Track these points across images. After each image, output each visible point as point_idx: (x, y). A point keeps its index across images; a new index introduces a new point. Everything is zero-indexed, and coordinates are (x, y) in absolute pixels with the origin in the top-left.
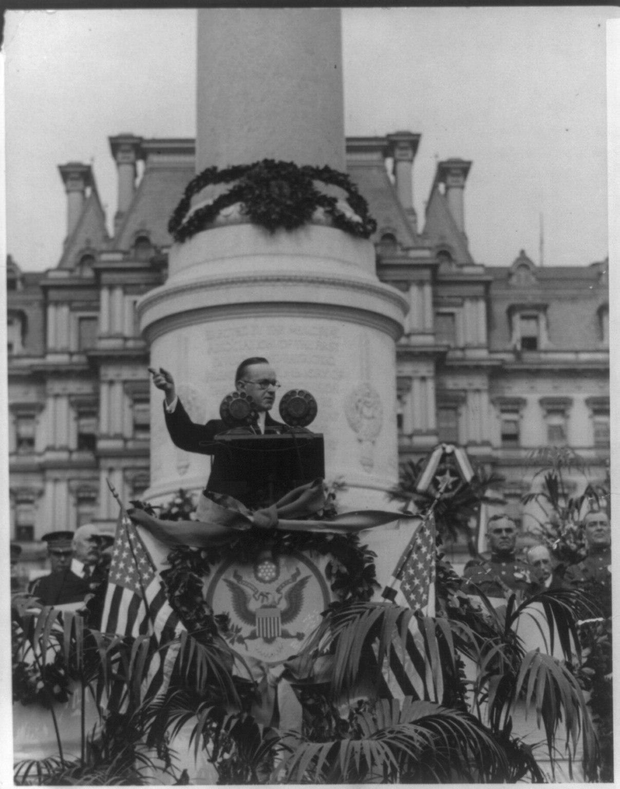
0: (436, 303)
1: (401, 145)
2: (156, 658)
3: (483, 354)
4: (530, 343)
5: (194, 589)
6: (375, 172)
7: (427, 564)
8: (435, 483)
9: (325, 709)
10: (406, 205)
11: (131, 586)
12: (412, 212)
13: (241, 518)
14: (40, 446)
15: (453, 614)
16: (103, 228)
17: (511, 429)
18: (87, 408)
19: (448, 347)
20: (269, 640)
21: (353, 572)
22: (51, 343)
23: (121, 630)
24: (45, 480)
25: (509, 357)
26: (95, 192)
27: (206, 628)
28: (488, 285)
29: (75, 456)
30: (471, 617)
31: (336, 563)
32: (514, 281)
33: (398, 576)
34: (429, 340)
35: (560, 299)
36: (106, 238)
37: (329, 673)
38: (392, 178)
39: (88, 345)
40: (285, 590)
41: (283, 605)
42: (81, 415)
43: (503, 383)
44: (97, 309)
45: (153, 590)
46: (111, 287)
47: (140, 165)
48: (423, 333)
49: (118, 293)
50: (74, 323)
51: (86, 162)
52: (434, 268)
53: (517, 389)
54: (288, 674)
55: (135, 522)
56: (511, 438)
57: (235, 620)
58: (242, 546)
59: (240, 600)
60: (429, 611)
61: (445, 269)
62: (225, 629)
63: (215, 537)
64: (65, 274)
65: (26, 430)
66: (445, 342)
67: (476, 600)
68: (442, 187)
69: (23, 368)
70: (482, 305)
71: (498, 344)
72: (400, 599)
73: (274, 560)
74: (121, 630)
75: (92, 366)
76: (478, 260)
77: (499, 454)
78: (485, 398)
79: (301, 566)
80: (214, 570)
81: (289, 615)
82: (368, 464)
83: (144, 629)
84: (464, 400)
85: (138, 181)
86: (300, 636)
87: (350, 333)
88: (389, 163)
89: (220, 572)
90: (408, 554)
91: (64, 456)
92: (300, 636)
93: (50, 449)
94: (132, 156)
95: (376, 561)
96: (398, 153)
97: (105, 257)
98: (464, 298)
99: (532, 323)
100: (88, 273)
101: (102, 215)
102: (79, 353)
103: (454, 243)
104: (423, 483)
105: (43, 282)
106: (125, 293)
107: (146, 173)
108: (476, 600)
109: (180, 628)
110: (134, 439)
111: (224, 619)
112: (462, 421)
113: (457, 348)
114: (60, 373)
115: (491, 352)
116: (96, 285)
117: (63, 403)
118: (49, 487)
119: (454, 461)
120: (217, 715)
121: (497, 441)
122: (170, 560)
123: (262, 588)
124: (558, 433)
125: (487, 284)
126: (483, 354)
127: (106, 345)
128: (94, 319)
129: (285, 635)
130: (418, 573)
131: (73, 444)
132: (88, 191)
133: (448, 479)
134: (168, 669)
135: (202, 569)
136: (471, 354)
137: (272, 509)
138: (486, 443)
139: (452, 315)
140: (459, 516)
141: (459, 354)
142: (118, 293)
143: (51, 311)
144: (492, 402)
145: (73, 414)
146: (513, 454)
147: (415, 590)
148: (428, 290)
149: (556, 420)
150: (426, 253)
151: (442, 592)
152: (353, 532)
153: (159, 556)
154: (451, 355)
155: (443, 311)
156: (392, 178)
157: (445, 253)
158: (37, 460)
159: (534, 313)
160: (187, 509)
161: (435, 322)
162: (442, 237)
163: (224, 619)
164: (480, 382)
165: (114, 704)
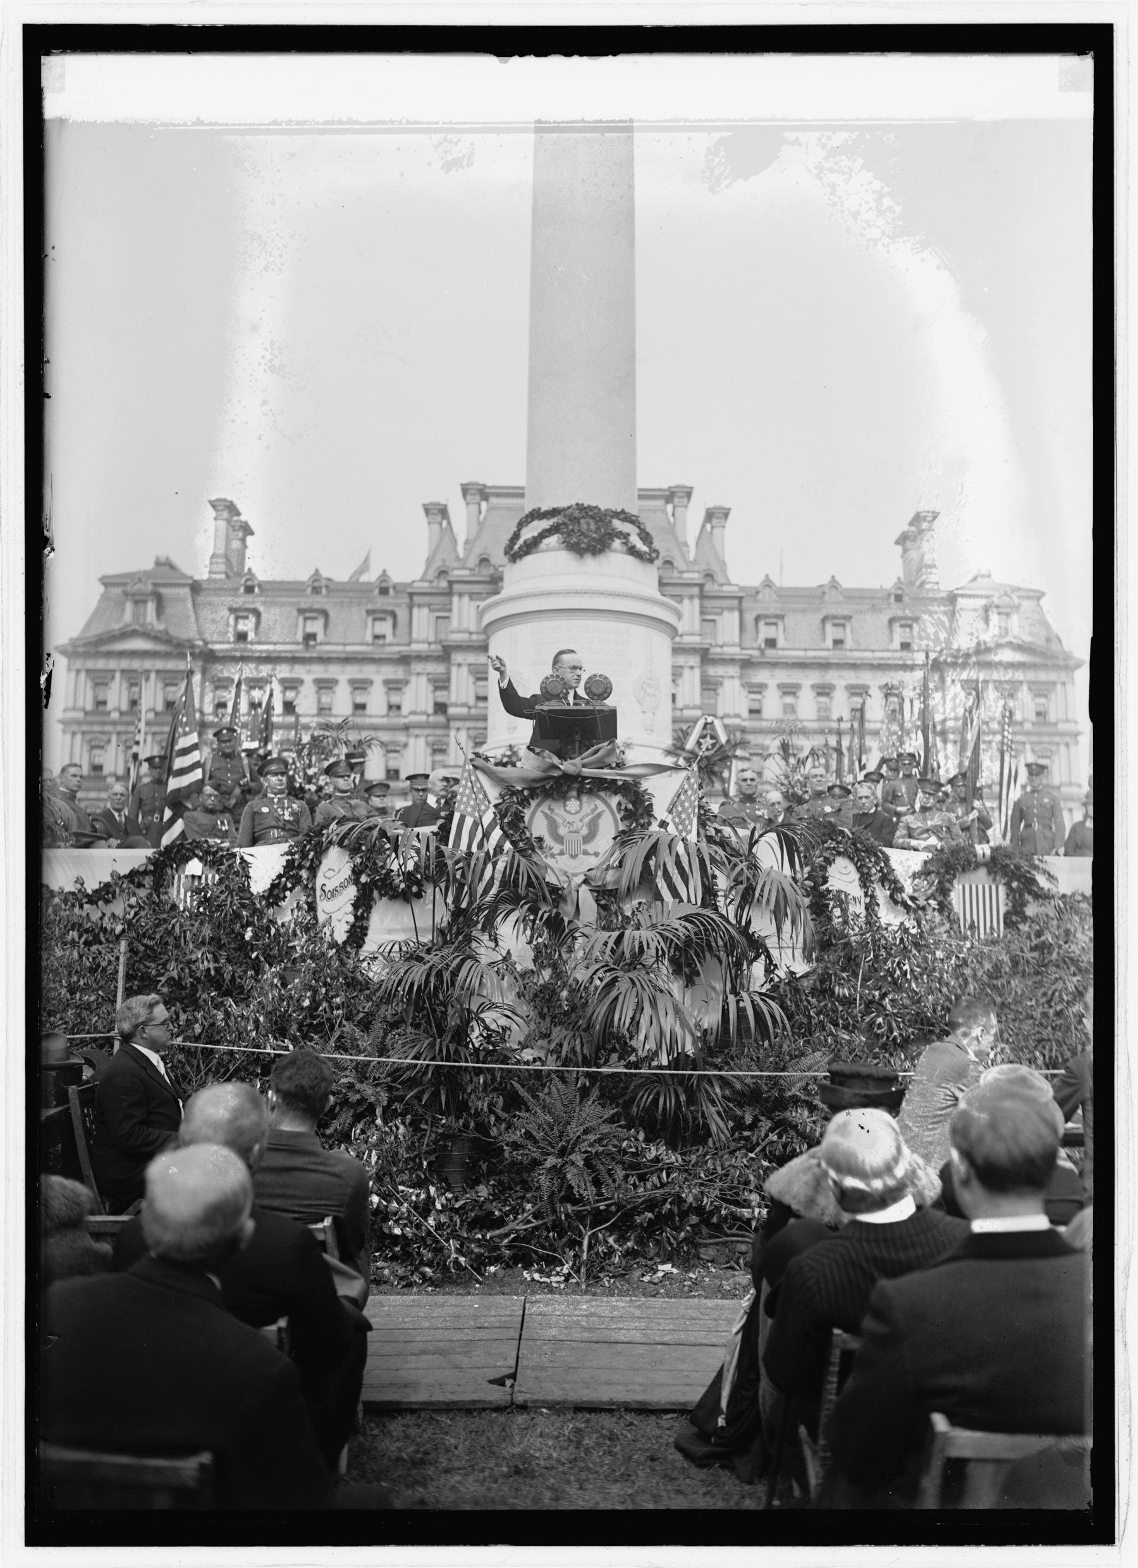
0: (702, 613)
2: (490, 867)
3: (737, 650)
4: (771, 643)
5: (519, 817)
6: (659, 514)
7: (691, 803)
8: (699, 744)
9: (614, 908)
10: (681, 539)
12: (686, 544)
13: (554, 767)
14: (405, 710)
15: (710, 840)
16: (456, 552)
17: (756, 706)
18: (441, 684)
20: (574, 857)
21: (637, 808)
22: (415, 635)
23: (463, 846)
24: (408, 736)
25: (755, 653)
26: (449, 523)
27: (527, 846)
29: (432, 719)
30: (723, 843)
31: (624, 802)
32: (760, 596)
33: (670, 812)
34: (697, 639)
35: (795, 611)
36: (457, 558)
37: (618, 881)
38: (672, 519)
39: (443, 637)
41: (585, 831)
42: (436, 688)
43: (750, 672)
44: (450, 610)
45: (488, 818)
46: (461, 595)
47: (484, 504)
49: (466, 599)
50: (433, 620)
51: (443, 502)
52: (701, 586)
53: (760, 676)
54: (586, 882)
56: (755, 712)
57: (548, 841)
58: (555, 787)
59: (553, 826)
60: (692, 838)
61: (710, 587)
62: (541, 848)
63: (534, 780)
64: (426, 584)
65: (395, 699)
66: (709, 641)
67: (727, 831)
68: (708, 526)
69: (394, 654)
70: (736, 614)
71: (747, 644)
72: (671, 828)
73: (578, 798)
74: (463, 846)
75: (445, 654)
76: (733, 581)
77: (747, 724)
78: (737, 682)
79: (598, 802)
80: (534, 803)
81: (588, 839)
82: (650, 730)
83: (481, 846)
84: (721, 684)
85: (482, 517)
86: (596, 854)
87: (639, 633)
88: (670, 507)
89: (538, 805)
91: (423, 718)
92: (596, 854)
93: (412, 713)
94: (478, 498)
95: (654, 801)
96: (676, 500)
97: (456, 572)
98: (723, 609)
99: (773, 628)
100: (444, 584)
101: (455, 542)
102: (435, 643)
103: (715, 568)
104: (690, 744)
105: (409, 590)
106: (471, 599)
107: (488, 511)
108: (727, 831)
109: (508, 846)
110: (476, 707)
111: (540, 840)
112: (720, 698)
113: (717, 646)
114: (421, 658)
116: (449, 593)
117: (423, 679)
118: (412, 741)
119: (714, 729)
120: (534, 910)
121: (745, 714)
122: (502, 796)
123: (569, 818)
124: (790, 709)
125: (740, 599)
128: (448, 618)
129: (586, 853)
130: (685, 810)
131: (430, 710)
132: (445, 523)
133: (708, 742)
134: (498, 876)
135: (524, 802)
136: (726, 650)
137: (578, 761)
138: (737, 716)
139: (714, 621)
140: (716, 769)
141: (718, 650)
142: (466, 599)
143: (415, 611)
144: (742, 685)
145: (431, 688)
146: (756, 724)
147: (682, 822)
148: (696, 602)
149: (789, 700)
150: (696, 575)
151: (702, 824)
154: (712, 650)
156: (672, 519)
157: (709, 576)
158: (403, 721)
159: (774, 620)
160: (514, 759)
161: (701, 626)
162: (708, 564)
163: (540, 840)
164: (734, 670)
165: (457, 900)
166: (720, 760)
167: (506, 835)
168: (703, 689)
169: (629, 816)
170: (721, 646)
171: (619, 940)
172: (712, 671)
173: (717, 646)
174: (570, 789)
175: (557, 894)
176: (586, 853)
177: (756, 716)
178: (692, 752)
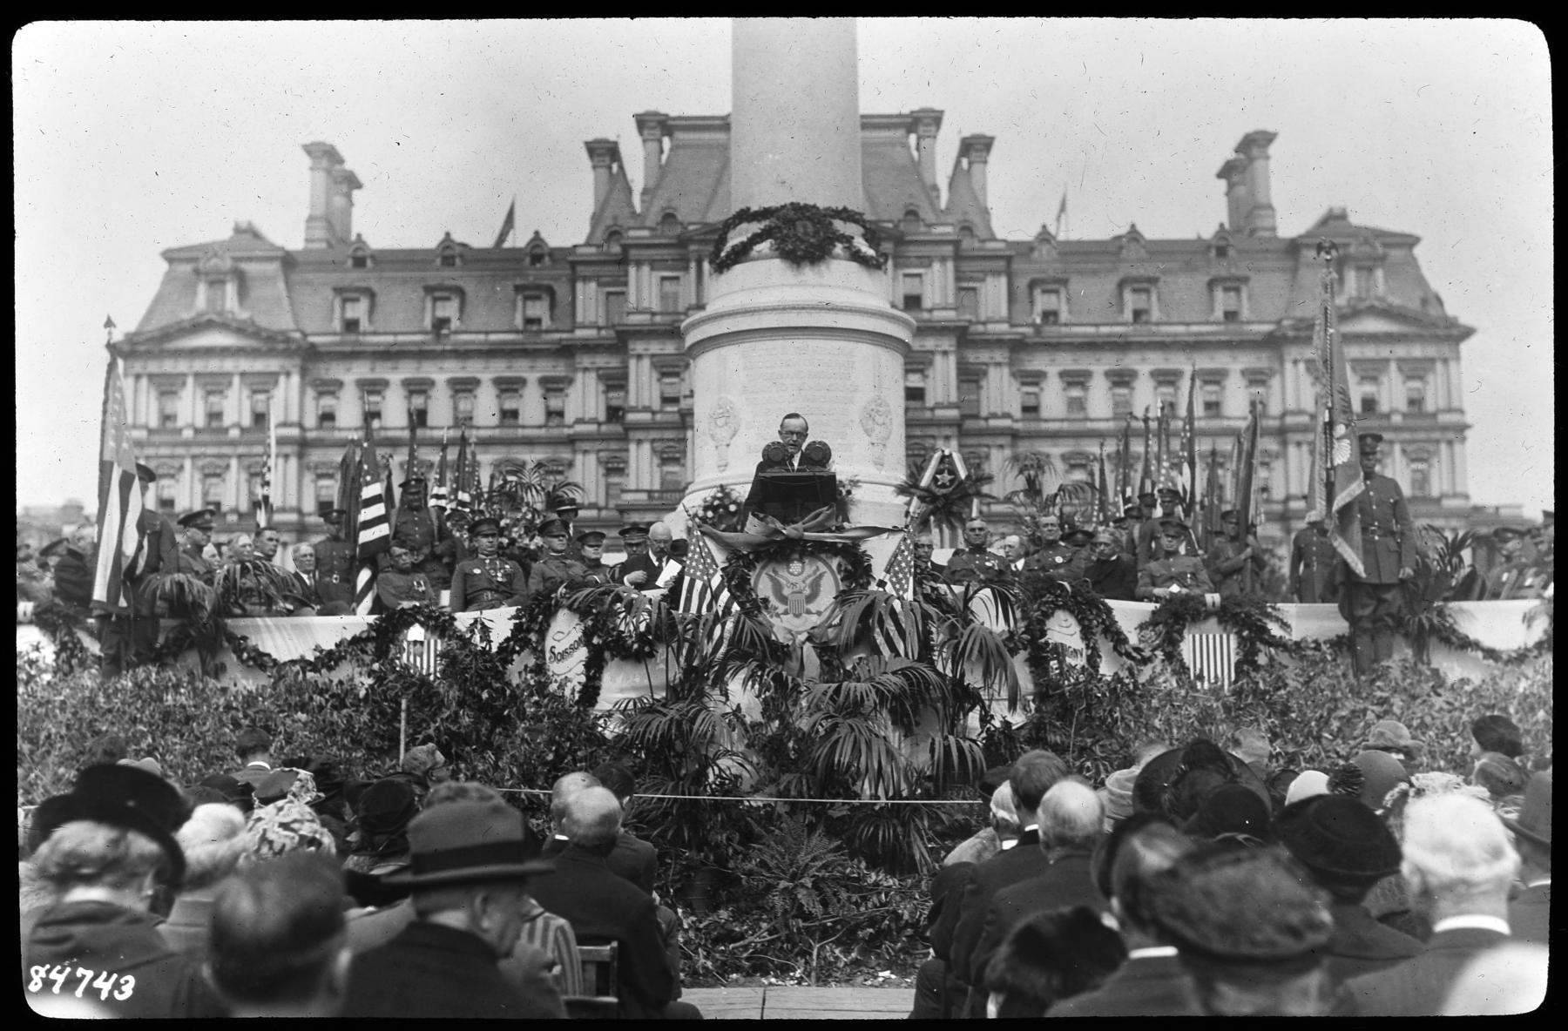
0: (958, 279)
1: (924, 122)
2: (718, 629)
3: (1005, 327)
4: (1050, 316)
5: (745, 580)
6: (899, 149)
7: (908, 563)
8: (935, 480)
9: (835, 663)
10: (929, 181)
11: (701, 578)
12: (935, 188)
14: (569, 418)
15: (927, 597)
16: (630, 204)
17: (1031, 402)
18: (615, 381)
19: (970, 321)
20: (797, 616)
21: (856, 569)
22: (579, 318)
23: (694, 609)
24: (574, 452)
25: (1028, 331)
26: (621, 167)
27: (754, 607)
28: (1009, 259)
29: (604, 428)
30: (937, 600)
31: (844, 562)
32: (1036, 255)
33: (888, 571)
34: (951, 314)
35: (1080, 273)
36: (633, 214)
37: (836, 638)
38: (915, 154)
39: (616, 321)
40: (809, 581)
41: (807, 591)
42: (609, 388)
43: (1023, 356)
44: (626, 284)
45: (716, 581)
46: (639, 263)
47: (666, 142)
48: (944, 309)
49: (646, 269)
50: (602, 298)
51: (612, 138)
52: (956, 244)
53: (1038, 362)
54: (809, 639)
55: (703, 533)
56: (1031, 410)
57: (773, 601)
58: (778, 551)
59: (777, 588)
60: (909, 596)
61: (968, 244)
62: (766, 608)
63: (760, 545)
64: (593, 250)
65: (555, 403)
66: (968, 317)
67: (943, 588)
68: (965, 162)
69: (552, 342)
70: (1003, 280)
71: (1018, 319)
72: (889, 588)
73: (801, 560)
74: (694, 609)
75: (620, 341)
76: (1000, 235)
77: (1019, 426)
78: (1006, 371)
79: (820, 564)
80: (759, 566)
81: (811, 598)
82: (879, 464)
83: (710, 607)
84: (985, 373)
85: (664, 157)
86: (819, 613)
87: (864, 350)
88: (913, 138)
89: (763, 568)
90: (895, 556)
91: (593, 428)
92: (819, 613)
93: (580, 421)
94: (658, 132)
95: (872, 562)
96: (921, 129)
97: (632, 233)
98: (986, 273)
99: (1053, 298)
100: (616, 249)
101: (629, 191)
102: (606, 327)
103: (976, 219)
104: (924, 482)
105: (570, 258)
106: (652, 269)
107: (671, 150)
108: (943, 588)
109: (736, 607)
110: (661, 411)
111: (766, 600)
113: (979, 323)
114: (590, 348)
115: (1012, 326)
116: (623, 261)
117: (592, 376)
118: (579, 458)
119: (952, 463)
120: (762, 667)
121: (1018, 414)
122: (728, 560)
123: (792, 579)
124: (1078, 405)
125: (1009, 259)
126: (1005, 327)
127: (635, 319)
128: (623, 293)
129: (809, 612)
130: (902, 570)
131: (602, 417)
132: (615, 167)
133: (946, 477)
134: (727, 635)
135: (750, 565)
136: (991, 327)
138: (1007, 416)
139: (974, 289)
140: (955, 509)
141: (980, 328)
142: (646, 269)
143: (579, 286)
144: (1013, 375)
145: (601, 387)
146: (1033, 426)
147: (899, 581)
148: (950, 265)
149: (1076, 393)
150: (949, 229)
151: (918, 583)
152: (856, 541)
153: (720, 558)
154: (972, 329)
155: (965, 286)
156: (915, 154)
157: (967, 229)
158: (566, 431)
159: (1055, 287)
160: (726, 502)
161: (956, 298)
162: (966, 213)
163: (766, 600)
164: (1000, 355)
165: (689, 659)
166: (960, 498)
167: (733, 598)
168: (960, 381)
169: (848, 576)
170: (984, 323)
171: (837, 691)
172: (972, 356)
173: (979, 323)
174: (793, 551)
175: (780, 653)
176: (809, 612)
177: (1033, 415)
178: (927, 490)
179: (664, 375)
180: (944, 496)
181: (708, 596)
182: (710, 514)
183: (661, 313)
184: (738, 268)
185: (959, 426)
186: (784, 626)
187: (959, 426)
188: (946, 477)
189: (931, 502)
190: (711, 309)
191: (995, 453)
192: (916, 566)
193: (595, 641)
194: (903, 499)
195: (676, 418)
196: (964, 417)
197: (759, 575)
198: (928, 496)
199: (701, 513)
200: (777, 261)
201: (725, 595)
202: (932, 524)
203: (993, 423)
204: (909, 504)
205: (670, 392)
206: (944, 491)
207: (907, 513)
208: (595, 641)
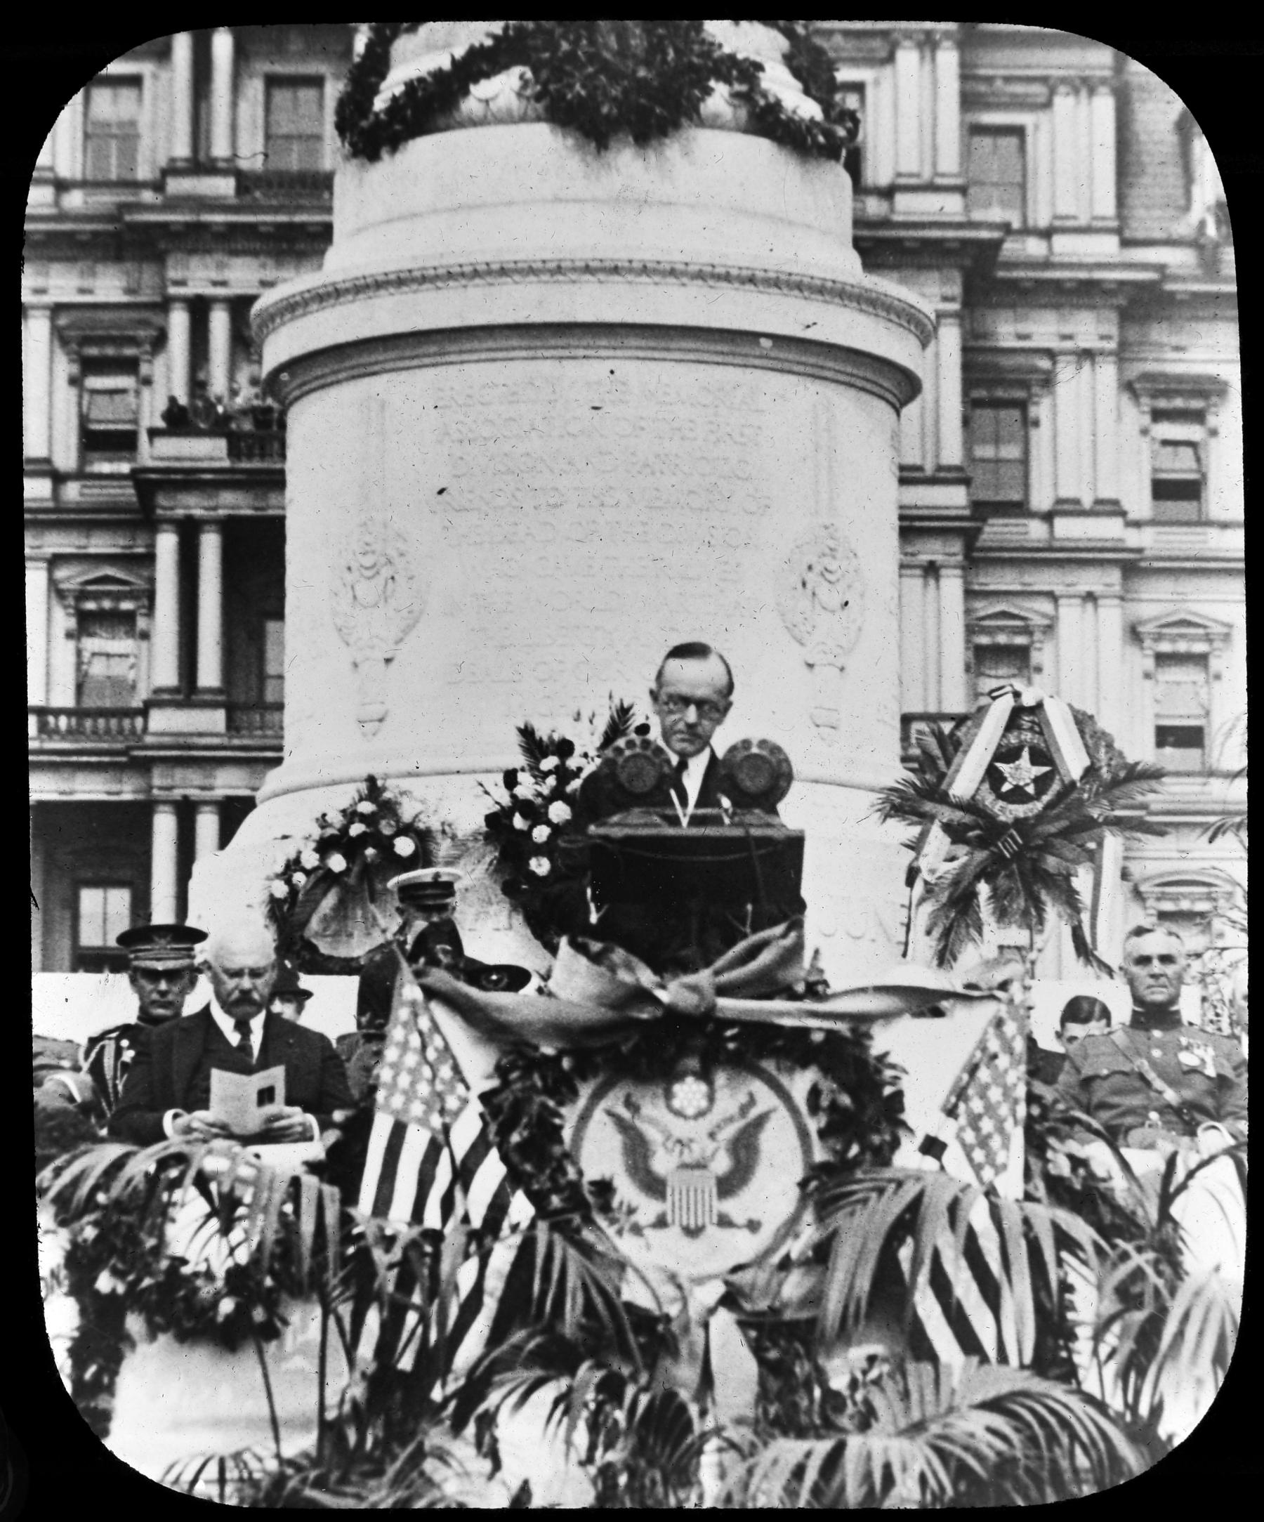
0: (969, 101)
3: (1105, 247)
7: (1007, 1092)
8: (993, 776)
9: (801, 1369)
11: (423, 1122)
13: (642, 996)
17: (1180, 466)
19: (1006, 228)
20: (693, 1232)
31: (827, 1085)
33: (951, 1112)
34: (951, 206)
40: (730, 1132)
43: (1158, 333)
48: (931, 188)
54: (731, 1299)
55: (430, 993)
57: (626, 1191)
58: (638, 1049)
59: (637, 1150)
60: (1011, 1186)
62: (606, 1209)
66: (996, 214)
67: (1099, 1155)
72: (953, 1156)
73: (705, 1075)
78: (1107, 372)
79: (759, 1088)
80: (585, 1091)
81: (728, 1186)
84: (1048, 381)
86: (753, 1226)
90: (973, 1070)
92: (753, 1226)
95: (905, 1084)
104: (966, 780)
109: (521, 1209)
110: (80, 475)
111: (604, 1188)
112: (1040, 437)
115: (1126, 243)
121: (1140, 502)
122: (501, 1071)
126: (1105, 247)
129: (725, 1222)
130: (990, 1109)
135: (564, 1089)
136: (1064, 246)
137: (704, 977)
139: (1018, 132)
140: (1051, 863)
141: (1034, 248)
144: (1129, 387)
147: (983, 1142)
151: (1036, 1144)
153: (478, 1064)
160: (386, 829)
161: (966, 154)
163: (604, 1188)
165: (386, 1348)
166: (1065, 834)
167: (515, 1179)
168: (971, 404)
169: (840, 1126)
170: (1047, 234)
171: (833, 1460)
172: (1006, 331)
173: (1026, 231)
174: (683, 1052)
175: (652, 1336)
176: (725, 1222)
177: (1184, 509)
178: (972, 806)
179: (90, 366)
180: (1019, 823)
181: (443, 1174)
182: (337, 863)
183: (83, 184)
184: (421, 149)
185: (969, 537)
186: (665, 1261)
187: (969, 537)
188: (1023, 772)
189: (980, 843)
190: (339, 262)
191: (1070, 615)
192: (1032, 1098)
193: (105, 1283)
194: (905, 830)
195: (127, 493)
196: (982, 510)
197: (584, 1118)
198: (975, 827)
199: (310, 859)
200: (543, 129)
201: (492, 1171)
202: (985, 910)
203: (1066, 528)
204: (916, 846)
205: (107, 416)
206: (1020, 810)
207: (912, 874)
208: (105, 1283)
